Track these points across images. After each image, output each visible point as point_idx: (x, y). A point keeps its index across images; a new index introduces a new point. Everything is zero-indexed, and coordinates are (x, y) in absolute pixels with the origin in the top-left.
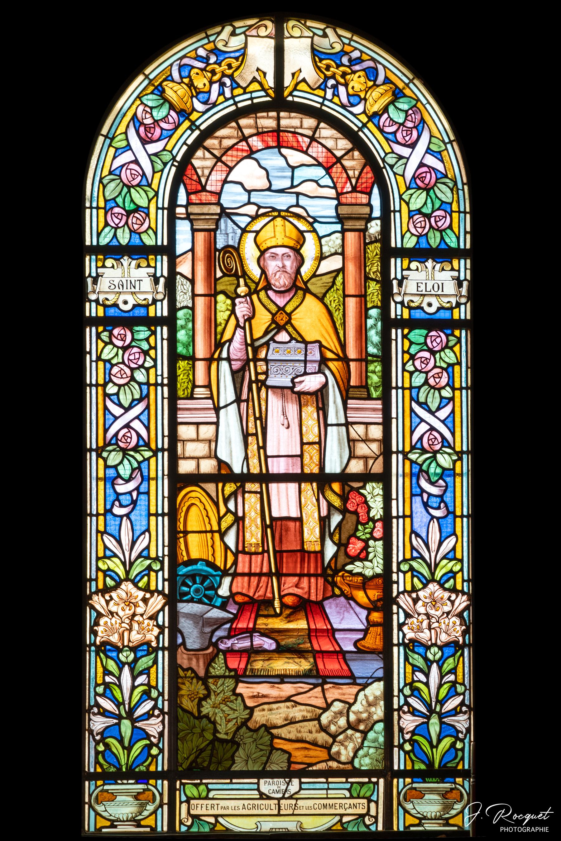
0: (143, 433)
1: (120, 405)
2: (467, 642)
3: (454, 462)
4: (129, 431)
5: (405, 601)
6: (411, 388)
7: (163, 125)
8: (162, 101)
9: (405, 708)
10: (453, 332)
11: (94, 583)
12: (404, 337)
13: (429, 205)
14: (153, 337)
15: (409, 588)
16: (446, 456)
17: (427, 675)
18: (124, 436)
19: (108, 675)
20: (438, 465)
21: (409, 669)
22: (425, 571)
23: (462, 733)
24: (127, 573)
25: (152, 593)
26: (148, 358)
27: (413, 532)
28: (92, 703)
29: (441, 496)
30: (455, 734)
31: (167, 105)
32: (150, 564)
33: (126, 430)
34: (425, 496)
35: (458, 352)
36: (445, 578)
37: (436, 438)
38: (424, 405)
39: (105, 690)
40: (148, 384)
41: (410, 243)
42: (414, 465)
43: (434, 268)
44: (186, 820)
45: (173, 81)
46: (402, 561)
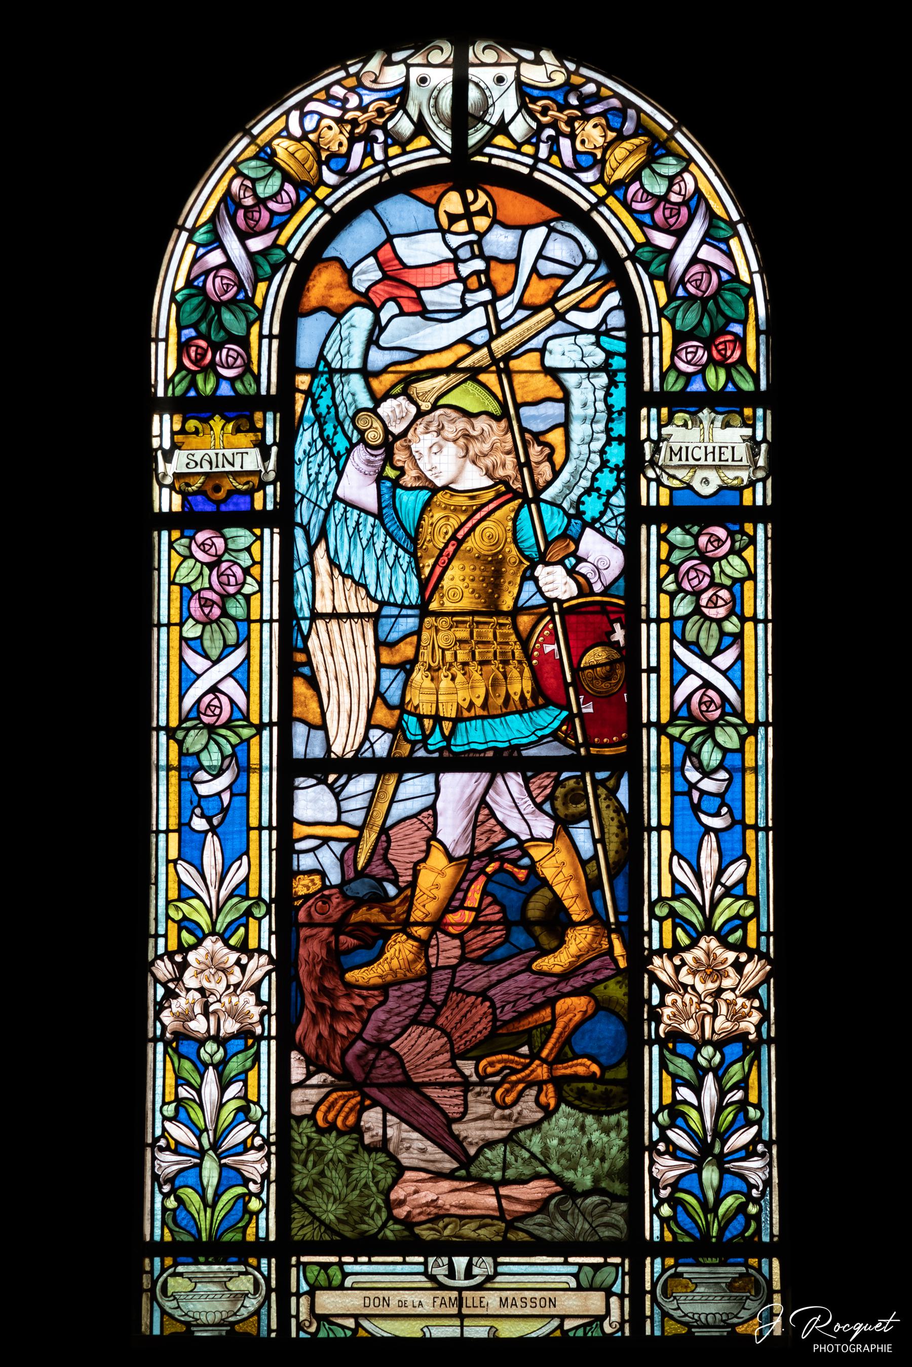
0: (240, 699)
1: (206, 656)
2: (765, 1036)
3: (743, 739)
4: (217, 697)
5: (662, 967)
6: (672, 619)
7: (272, 205)
8: (270, 169)
9: (662, 1147)
10: (742, 527)
11: (161, 941)
12: (661, 537)
13: (706, 322)
14: (258, 542)
15: (668, 944)
16: (730, 730)
17: (697, 1090)
18: (209, 705)
19: (182, 1085)
20: (717, 744)
21: (667, 1079)
22: (696, 918)
23: (757, 1188)
24: (214, 924)
25: (250, 954)
26: (249, 580)
27: (674, 852)
28: (158, 1132)
29: (721, 795)
30: (745, 1190)
31: (278, 174)
32: (250, 907)
33: (211, 696)
34: (696, 795)
35: (754, 560)
36: (727, 928)
37: (712, 701)
38: (693, 646)
39: (177, 1110)
40: (249, 621)
41: (674, 385)
42: (676, 744)
43: (712, 423)
44: (307, 1324)
45: (290, 137)
46: (657, 901)
